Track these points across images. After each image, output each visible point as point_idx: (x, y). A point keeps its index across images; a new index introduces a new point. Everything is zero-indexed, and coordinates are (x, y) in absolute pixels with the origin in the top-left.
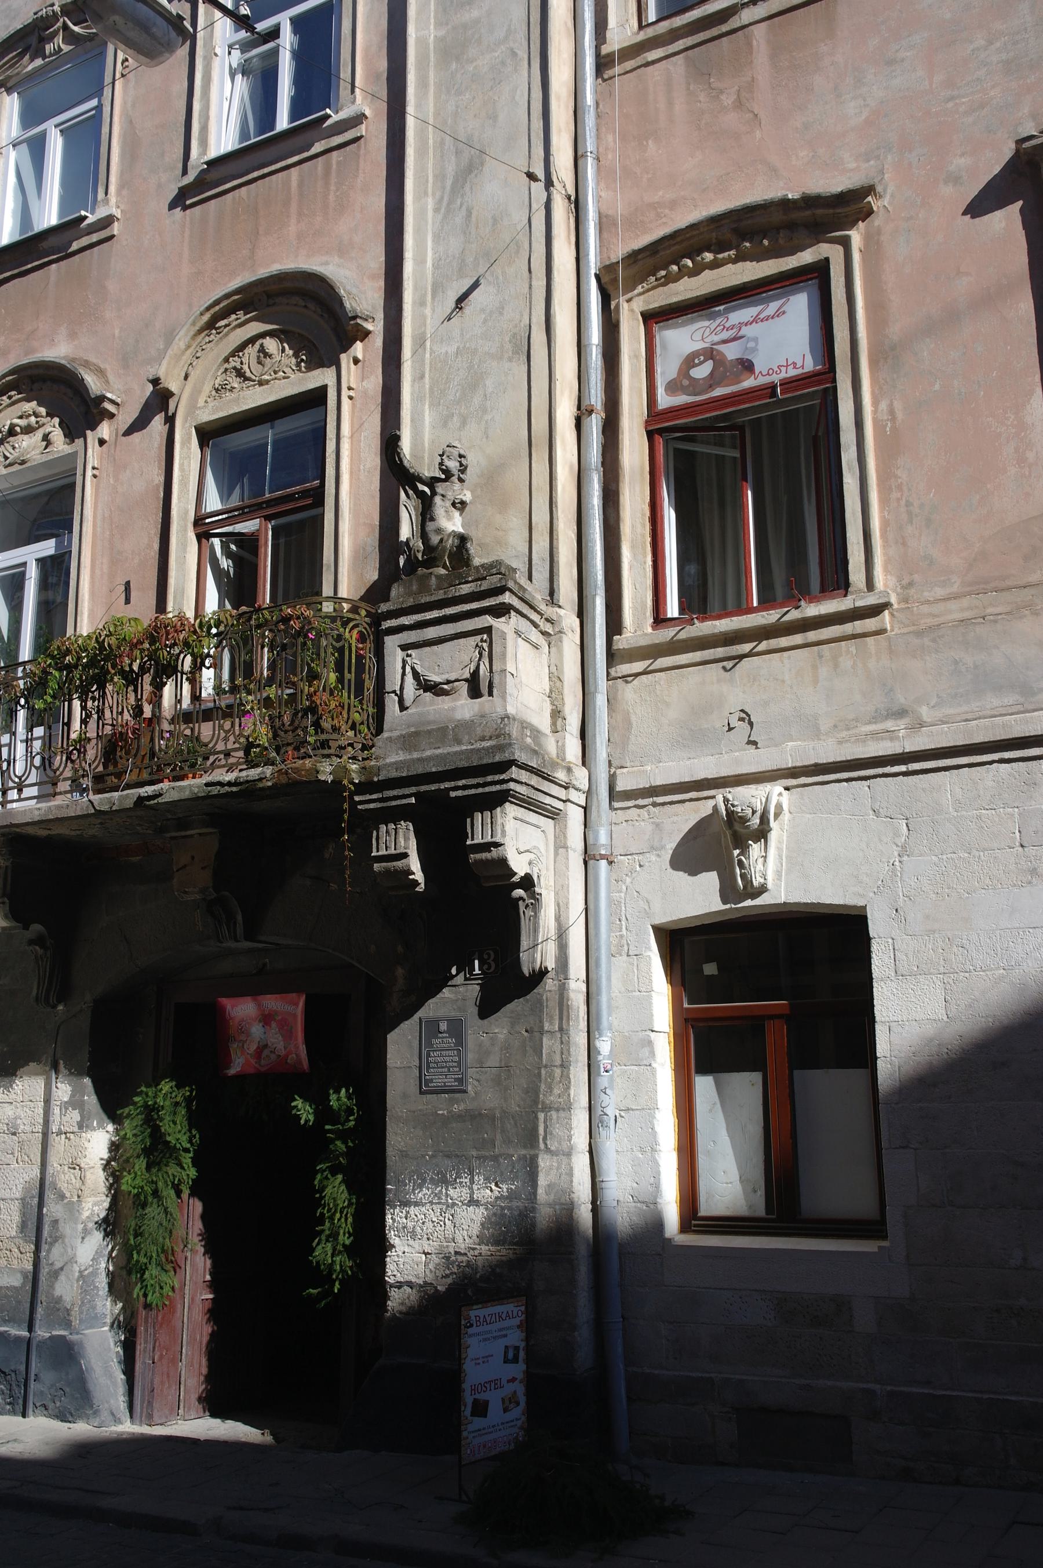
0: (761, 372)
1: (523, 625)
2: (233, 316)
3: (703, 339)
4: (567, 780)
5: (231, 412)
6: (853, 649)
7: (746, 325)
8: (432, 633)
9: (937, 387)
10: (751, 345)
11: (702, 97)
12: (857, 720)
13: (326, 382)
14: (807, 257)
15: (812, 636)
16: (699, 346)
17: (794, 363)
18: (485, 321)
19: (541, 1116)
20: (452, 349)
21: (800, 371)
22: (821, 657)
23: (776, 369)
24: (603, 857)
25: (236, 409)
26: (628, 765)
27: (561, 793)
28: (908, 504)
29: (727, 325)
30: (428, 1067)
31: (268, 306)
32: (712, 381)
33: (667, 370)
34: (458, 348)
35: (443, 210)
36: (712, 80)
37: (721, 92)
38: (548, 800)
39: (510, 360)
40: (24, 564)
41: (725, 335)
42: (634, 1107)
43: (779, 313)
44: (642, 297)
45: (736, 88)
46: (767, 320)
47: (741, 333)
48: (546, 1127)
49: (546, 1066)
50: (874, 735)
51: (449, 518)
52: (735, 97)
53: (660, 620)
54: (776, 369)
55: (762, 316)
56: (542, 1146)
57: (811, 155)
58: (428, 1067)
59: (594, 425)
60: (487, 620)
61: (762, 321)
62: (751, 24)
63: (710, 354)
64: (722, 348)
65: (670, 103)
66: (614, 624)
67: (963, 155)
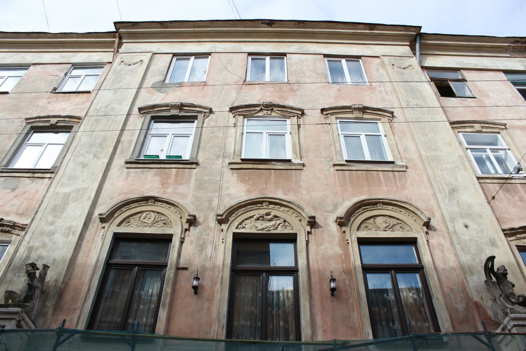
18: (477, 233)
39: (492, 246)
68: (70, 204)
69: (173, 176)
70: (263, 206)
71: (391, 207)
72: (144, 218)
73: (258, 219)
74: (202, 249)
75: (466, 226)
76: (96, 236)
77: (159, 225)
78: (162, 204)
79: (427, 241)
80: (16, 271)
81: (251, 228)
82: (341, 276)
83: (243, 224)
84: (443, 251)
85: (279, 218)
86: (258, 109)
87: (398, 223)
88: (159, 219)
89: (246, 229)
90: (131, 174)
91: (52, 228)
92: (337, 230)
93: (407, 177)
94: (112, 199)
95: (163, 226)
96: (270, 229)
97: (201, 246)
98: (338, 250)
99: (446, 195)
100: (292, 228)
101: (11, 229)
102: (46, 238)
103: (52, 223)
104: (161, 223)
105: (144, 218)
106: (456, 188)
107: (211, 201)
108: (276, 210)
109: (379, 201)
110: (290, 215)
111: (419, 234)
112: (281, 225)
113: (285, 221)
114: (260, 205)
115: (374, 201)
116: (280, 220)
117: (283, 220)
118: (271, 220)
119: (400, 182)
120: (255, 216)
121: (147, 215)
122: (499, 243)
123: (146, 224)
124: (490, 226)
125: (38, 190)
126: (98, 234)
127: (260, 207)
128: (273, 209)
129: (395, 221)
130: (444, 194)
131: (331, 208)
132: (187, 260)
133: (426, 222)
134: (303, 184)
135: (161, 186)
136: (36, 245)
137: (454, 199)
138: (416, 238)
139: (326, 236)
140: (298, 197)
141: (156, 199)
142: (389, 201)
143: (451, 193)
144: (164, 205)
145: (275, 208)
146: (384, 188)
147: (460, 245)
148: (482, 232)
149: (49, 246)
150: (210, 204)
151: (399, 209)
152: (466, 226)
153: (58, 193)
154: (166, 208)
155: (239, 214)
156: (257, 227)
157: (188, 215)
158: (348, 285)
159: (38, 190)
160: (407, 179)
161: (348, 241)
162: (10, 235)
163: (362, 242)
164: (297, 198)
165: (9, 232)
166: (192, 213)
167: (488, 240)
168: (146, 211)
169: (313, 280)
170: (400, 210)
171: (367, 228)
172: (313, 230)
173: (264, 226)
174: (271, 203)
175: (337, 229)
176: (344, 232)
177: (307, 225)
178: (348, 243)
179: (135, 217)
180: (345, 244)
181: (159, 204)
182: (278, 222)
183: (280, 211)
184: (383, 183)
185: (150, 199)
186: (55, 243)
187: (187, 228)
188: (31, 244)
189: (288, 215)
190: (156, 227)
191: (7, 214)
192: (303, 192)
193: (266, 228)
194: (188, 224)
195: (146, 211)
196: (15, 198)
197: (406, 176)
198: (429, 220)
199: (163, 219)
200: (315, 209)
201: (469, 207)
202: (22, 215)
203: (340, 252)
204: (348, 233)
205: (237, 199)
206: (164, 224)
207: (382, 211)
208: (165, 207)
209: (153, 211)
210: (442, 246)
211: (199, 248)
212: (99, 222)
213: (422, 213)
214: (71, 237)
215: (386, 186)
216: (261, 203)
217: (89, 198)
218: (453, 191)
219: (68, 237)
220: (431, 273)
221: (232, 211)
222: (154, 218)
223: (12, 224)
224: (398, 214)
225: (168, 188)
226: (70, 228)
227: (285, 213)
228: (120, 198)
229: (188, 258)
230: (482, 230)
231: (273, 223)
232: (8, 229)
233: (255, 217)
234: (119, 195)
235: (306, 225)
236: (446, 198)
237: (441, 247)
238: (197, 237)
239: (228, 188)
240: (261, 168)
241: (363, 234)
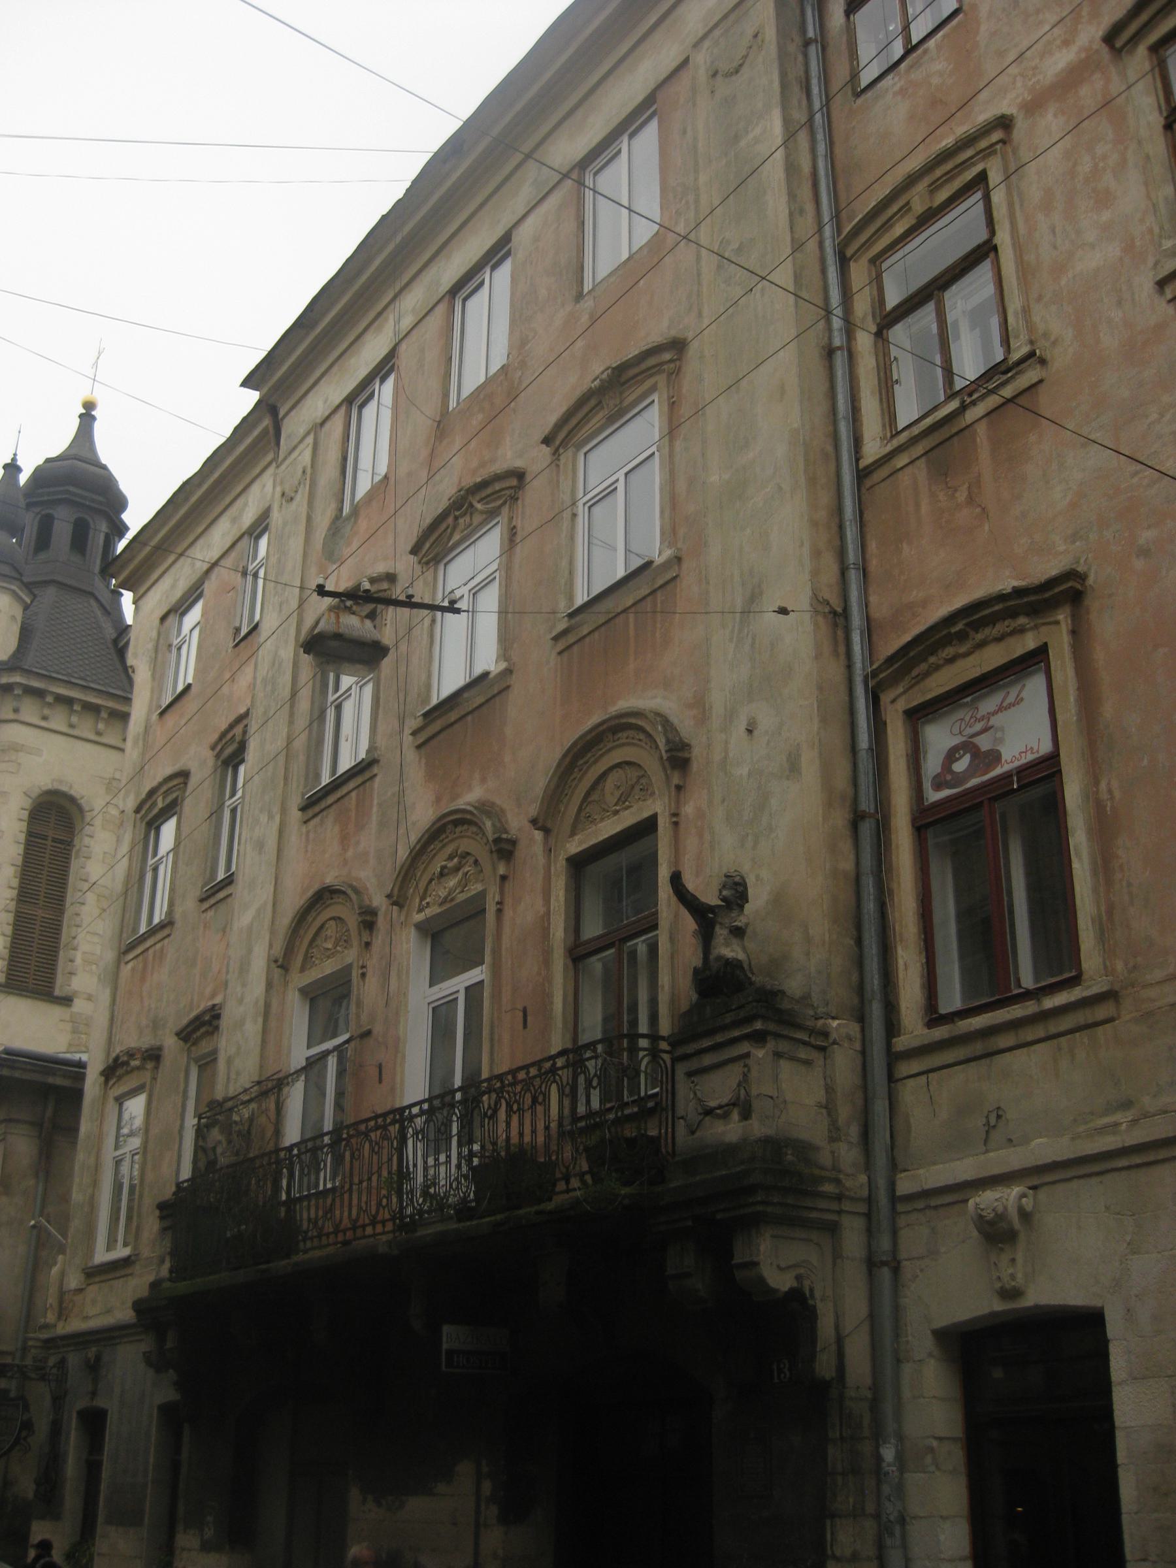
0: (1006, 761)
1: (784, 1046)
2: (589, 755)
3: (960, 733)
4: (837, 1191)
5: (591, 843)
6: (1086, 1040)
7: (993, 715)
8: (708, 1060)
9: (1145, 762)
10: (999, 735)
11: (941, 496)
12: (1092, 1113)
14: (1030, 642)
15: (1054, 1027)
16: (957, 740)
17: (1032, 748)
18: (768, 743)
19: (828, 1522)
20: (745, 771)
21: (1036, 756)
22: (1060, 1049)
23: (1018, 756)
24: (884, 1264)
25: (594, 841)
26: (910, 1168)
27: (834, 1206)
28: (1129, 885)
29: (978, 716)
31: (614, 741)
32: (971, 772)
33: (932, 765)
34: (750, 770)
35: (735, 639)
36: (948, 479)
37: (956, 490)
38: (814, 1215)
40: (458, 991)
41: (978, 727)
42: (922, 1515)
43: (1019, 701)
45: (966, 485)
46: (1009, 708)
47: (991, 723)
48: (832, 1534)
50: (1102, 1131)
51: (727, 945)
52: (967, 493)
53: (934, 1018)
54: (1018, 756)
55: (1005, 704)
56: (829, 1552)
57: (1029, 541)
59: (866, 828)
60: (744, 1047)
61: (1006, 709)
62: (974, 423)
63: (967, 746)
64: (976, 740)
65: (917, 505)
66: (892, 1027)
67: (1149, 527)
69: (353, 814)
86: (450, 520)
90: (312, 836)
109: (601, 728)
115: (593, 734)
142: (617, 721)
171: (590, 819)
240: (453, 719)
241: (575, 846)
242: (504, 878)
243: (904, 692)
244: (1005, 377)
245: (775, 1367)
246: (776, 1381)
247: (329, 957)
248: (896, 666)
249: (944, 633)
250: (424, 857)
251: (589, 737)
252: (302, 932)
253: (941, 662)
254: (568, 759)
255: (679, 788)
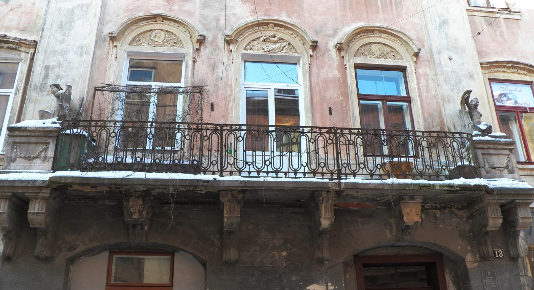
2: (366, 34)
13: (406, 65)
18: (459, 66)
30: (486, 286)
39: (469, 79)
44: (488, 74)
49: (523, 286)
55: (517, 90)
58: (486, 286)
68: (76, 22)
70: (268, 28)
71: (386, 36)
72: (154, 37)
73: (264, 41)
74: (214, 69)
75: (450, 59)
76: (109, 55)
77: (170, 45)
78: (170, 23)
79: (415, 70)
80: (38, 90)
81: (258, 50)
82: (339, 98)
83: (251, 45)
84: (427, 81)
85: (283, 41)
87: (391, 51)
88: (170, 38)
89: (254, 51)
91: (63, 46)
92: (337, 55)
93: (403, 5)
94: (118, 16)
95: (174, 45)
96: (276, 51)
97: (212, 66)
98: (337, 74)
99: (436, 27)
100: (296, 50)
101: (18, 46)
102: (60, 57)
103: (62, 42)
104: (172, 43)
105: (154, 37)
106: (447, 20)
107: (218, 20)
108: (280, 32)
109: (376, 28)
110: (294, 38)
111: (408, 62)
112: (286, 47)
113: (289, 44)
114: (266, 27)
115: (372, 28)
116: (284, 42)
117: (287, 43)
118: (275, 43)
119: (396, 11)
120: (261, 37)
121: (157, 33)
122: (476, 76)
123: (157, 43)
124: (471, 60)
125: (34, 4)
126: (110, 53)
127: (266, 29)
128: (278, 31)
129: (388, 49)
130: (435, 26)
131: (332, 32)
132: (200, 80)
133: (417, 52)
134: (305, 6)
135: (166, 3)
136: (52, 64)
137: (443, 31)
138: (406, 66)
139: (327, 60)
140: (300, 19)
141: (164, 18)
142: (385, 30)
143: (442, 25)
144: (173, 24)
145: (280, 30)
146: (381, 15)
147: (443, 76)
148: (463, 65)
149: (64, 65)
150: (217, 24)
151: (393, 38)
152: (450, 59)
153: (60, 8)
154: (175, 27)
155: (247, 35)
156: (264, 49)
157: (198, 35)
158: (344, 107)
159: (34, 4)
160: (402, 8)
161: (346, 66)
162: (19, 52)
163: (358, 67)
164: (300, 21)
165: (15, 49)
166: (201, 33)
167: (467, 73)
168: (155, 30)
169: (315, 101)
170: (394, 39)
171: (363, 54)
172: (315, 53)
173: (270, 49)
174: (276, 25)
175: (337, 53)
176: (343, 57)
177: (310, 49)
178: (346, 68)
179: (145, 36)
180: (343, 69)
181: (168, 22)
182: (283, 44)
183: (285, 33)
184: (380, 10)
185: (158, 17)
186: (70, 62)
187: (198, 48)
188: (46, 63)
189: (292, 37)
190: (168, 46)
191: (8, 29)
192: (306, 15)
193: (272, 50)
194: (198, 44)
195: (155, 30)
196: (11, 12)
197: (402, 5)
198: (419, 51)
199: (173, 38)
200: (317, 32)
201: (455, 40)
202: (24, 30)
203: (338, 76)
204: (346, 58)
205: (243, 19)
206: (175, 43)
207: (378, 39)
208: (174, 26)
209: (162, 30)
210: (428, 75)
211: (211, 68)
212: (110, 41)
213: (414, 43)
214: (84, 56)
215: (383, 13)
216: (267, 24)
217: (95, 15)
218: (444, 22)
219: (81, 56)
220: (416, 99)
221: (241, 31)
222: (164, 37)
223: (18, 41)
224: (391, 42)
225: (174, 5)
226: (82, 47)
227: (289, 35)
228: (126, 15)
229: (201, 77)
230: (463, 64)
231: (278, 45)
232: (14, 46)
233: (262, 39)
234: (125, 12)
235: (309, 48)
236: (436, 29)
237: (426, 77)
238: (208, 56)
239: (233, 7)
241: (360, 60)
242: (311, 56)
243: (488, 73)
244: (509, 13)
245: (496, 252)
246: (497, 256)
247: (157, 45)
248: (489, 65)
249: (505, 64)
250: (251, 30)
251: (369, 28)
252: (133, 28)
253: (501, 71)
254: (358, 31)
255: (415, 62)
